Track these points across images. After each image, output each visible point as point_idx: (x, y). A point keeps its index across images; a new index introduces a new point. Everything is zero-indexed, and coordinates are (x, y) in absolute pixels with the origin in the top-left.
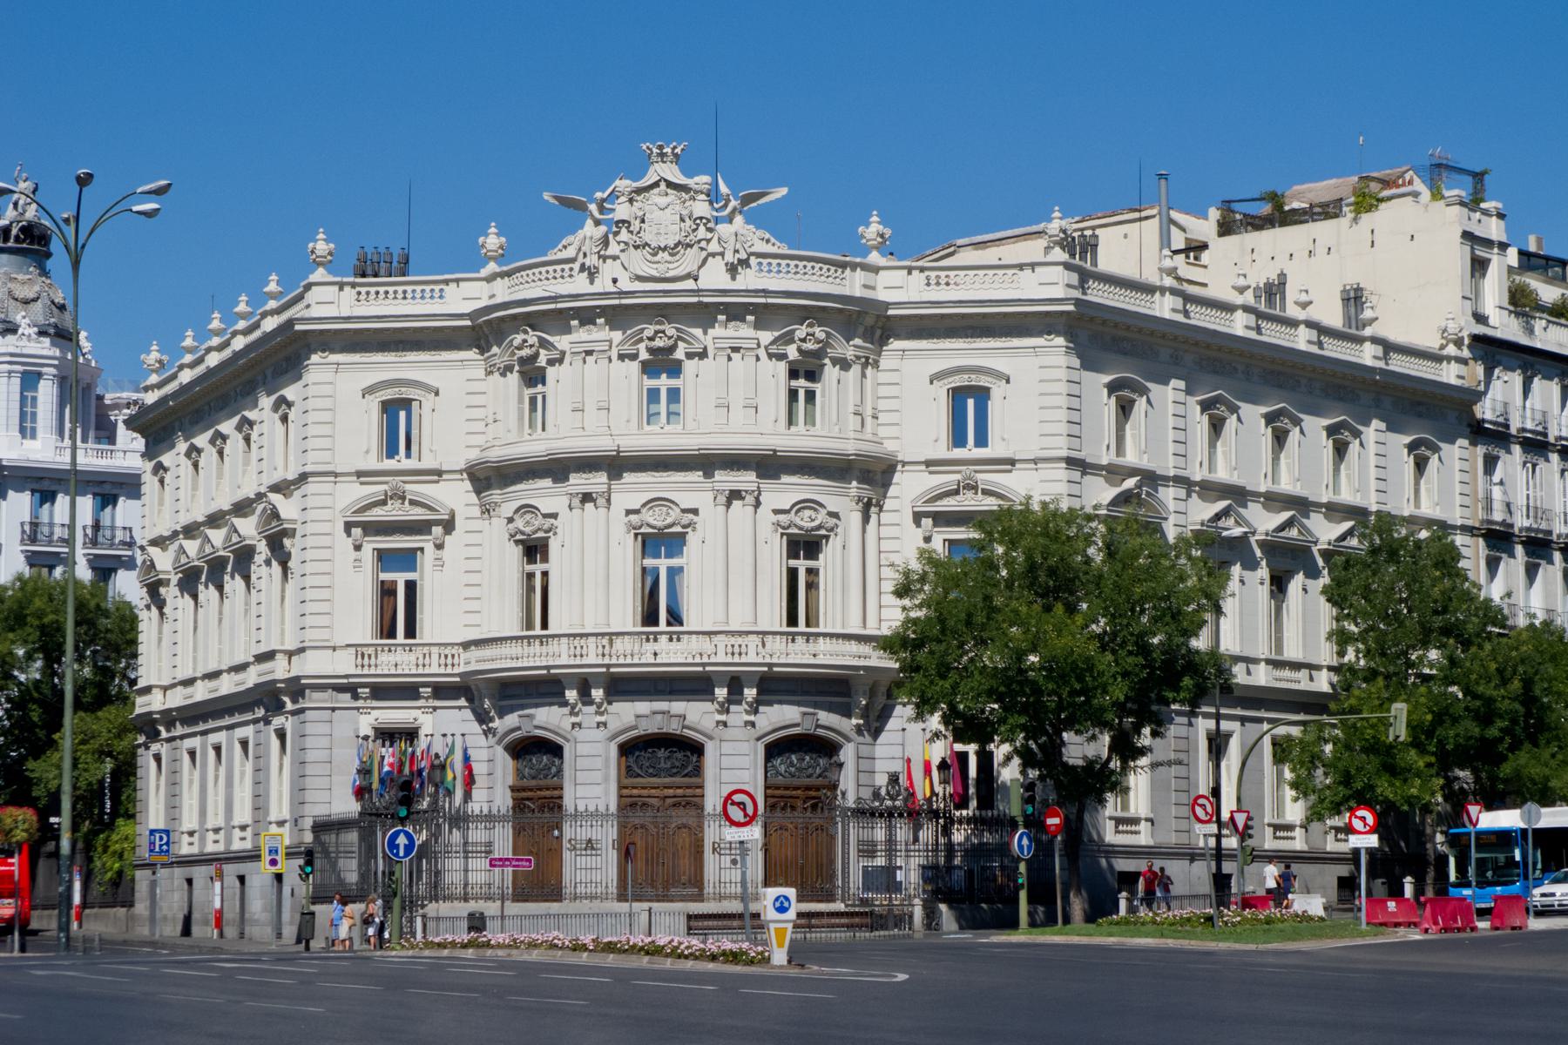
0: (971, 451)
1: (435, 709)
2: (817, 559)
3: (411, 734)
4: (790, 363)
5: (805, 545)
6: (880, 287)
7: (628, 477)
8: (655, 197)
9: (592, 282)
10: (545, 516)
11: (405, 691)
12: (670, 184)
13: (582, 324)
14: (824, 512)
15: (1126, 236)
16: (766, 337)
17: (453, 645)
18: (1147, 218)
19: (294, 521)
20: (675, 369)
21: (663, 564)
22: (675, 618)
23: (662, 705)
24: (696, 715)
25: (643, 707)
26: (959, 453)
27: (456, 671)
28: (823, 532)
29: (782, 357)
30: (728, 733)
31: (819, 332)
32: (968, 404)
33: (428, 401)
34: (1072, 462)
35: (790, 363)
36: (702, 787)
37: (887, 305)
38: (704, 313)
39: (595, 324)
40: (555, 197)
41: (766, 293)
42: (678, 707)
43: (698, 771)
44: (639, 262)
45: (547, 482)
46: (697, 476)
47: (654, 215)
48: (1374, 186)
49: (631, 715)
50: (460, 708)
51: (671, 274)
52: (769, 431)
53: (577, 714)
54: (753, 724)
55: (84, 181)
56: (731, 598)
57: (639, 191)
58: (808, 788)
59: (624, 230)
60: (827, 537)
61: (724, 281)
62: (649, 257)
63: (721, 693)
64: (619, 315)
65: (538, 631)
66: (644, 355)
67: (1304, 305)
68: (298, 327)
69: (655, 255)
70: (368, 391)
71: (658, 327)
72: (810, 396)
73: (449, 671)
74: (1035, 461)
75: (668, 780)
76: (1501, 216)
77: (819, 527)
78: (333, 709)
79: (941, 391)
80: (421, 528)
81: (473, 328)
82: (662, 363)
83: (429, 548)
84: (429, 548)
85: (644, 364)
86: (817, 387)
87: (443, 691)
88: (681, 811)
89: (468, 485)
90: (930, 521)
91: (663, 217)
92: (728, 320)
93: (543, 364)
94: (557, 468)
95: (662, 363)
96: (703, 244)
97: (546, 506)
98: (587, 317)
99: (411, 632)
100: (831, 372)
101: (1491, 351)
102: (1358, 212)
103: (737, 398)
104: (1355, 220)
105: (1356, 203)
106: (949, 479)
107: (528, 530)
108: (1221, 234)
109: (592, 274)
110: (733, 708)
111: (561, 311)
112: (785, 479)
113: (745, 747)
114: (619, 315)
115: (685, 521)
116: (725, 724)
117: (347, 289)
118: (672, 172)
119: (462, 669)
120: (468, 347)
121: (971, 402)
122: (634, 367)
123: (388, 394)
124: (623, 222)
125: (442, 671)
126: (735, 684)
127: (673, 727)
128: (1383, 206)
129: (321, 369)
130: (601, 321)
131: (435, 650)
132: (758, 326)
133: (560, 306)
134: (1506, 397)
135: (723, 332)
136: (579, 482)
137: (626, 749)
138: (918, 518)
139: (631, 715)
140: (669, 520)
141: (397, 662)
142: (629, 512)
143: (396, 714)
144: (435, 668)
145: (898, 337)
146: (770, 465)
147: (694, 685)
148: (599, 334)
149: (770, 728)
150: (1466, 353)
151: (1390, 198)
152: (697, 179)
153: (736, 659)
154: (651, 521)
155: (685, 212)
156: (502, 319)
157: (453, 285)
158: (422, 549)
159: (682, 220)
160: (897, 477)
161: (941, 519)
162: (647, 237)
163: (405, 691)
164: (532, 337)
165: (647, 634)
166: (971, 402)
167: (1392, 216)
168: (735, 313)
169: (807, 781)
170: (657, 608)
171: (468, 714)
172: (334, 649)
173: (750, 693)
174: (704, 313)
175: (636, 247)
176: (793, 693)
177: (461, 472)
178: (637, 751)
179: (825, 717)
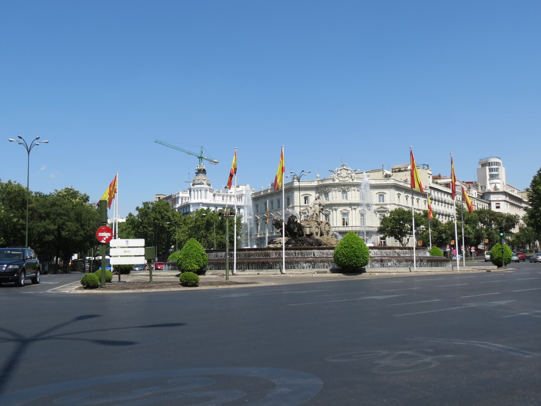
5: (362, 215)
12: (345, 169)
33: (310, 197)
44: (341, 179)
55: (303, 171)
61: (351, 181)
79: (378, 195)
95: (344, 192)
103: (354, 196)
106: (380, 206)
122: (341, 193)
134: (435, 194)
146: (358, 205)
161: (379, 212)
170: (345, 223)
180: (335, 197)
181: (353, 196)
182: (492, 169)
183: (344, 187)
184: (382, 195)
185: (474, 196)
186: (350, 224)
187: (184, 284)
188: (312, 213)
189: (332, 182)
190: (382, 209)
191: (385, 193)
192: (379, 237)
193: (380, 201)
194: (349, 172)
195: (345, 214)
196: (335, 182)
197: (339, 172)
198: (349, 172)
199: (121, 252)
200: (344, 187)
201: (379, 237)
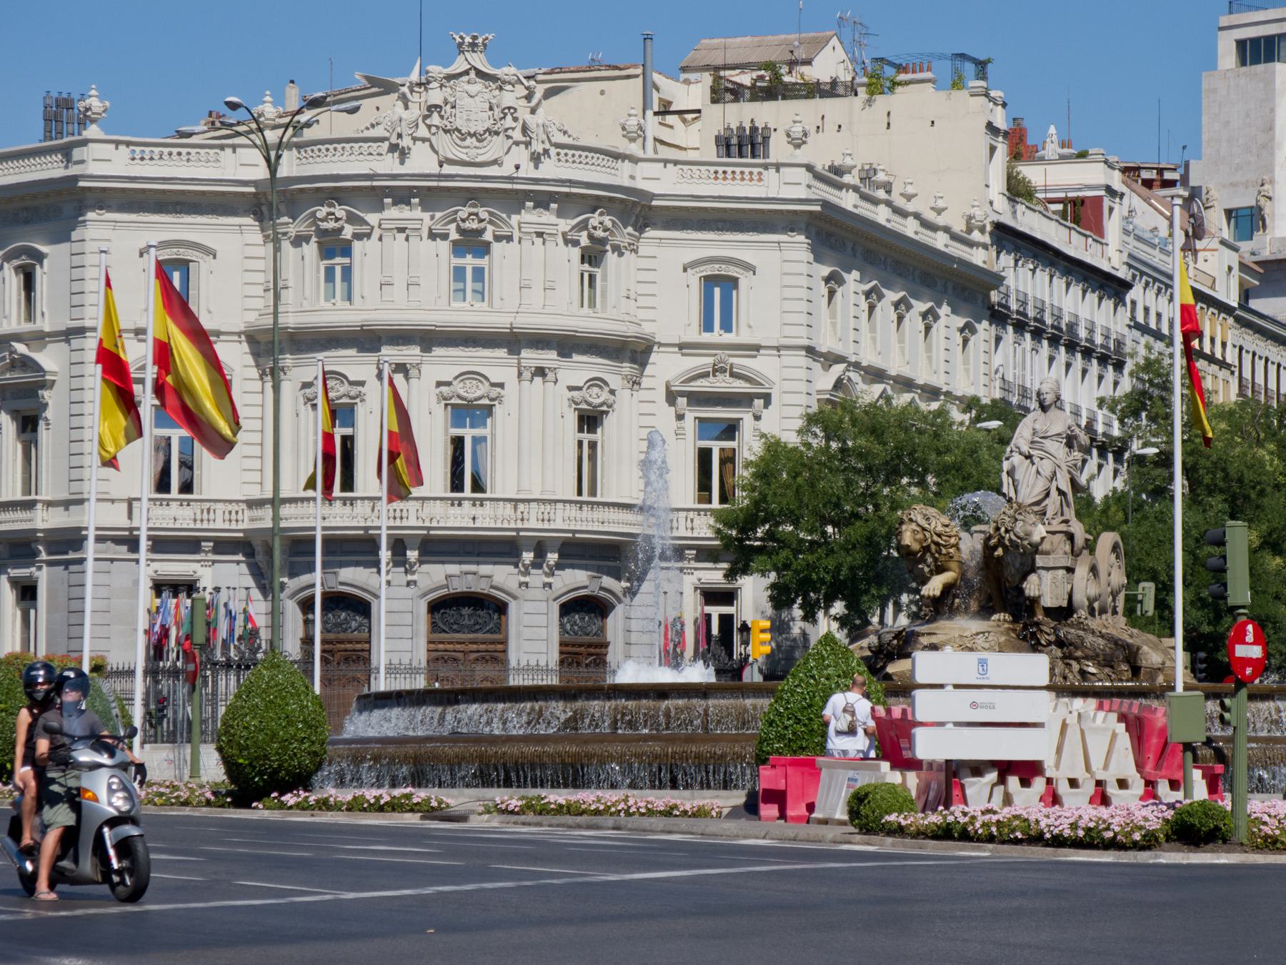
0: (718, 336)
1: (214, 562)
2: (485, 425)
3: (189, 587)
4: (583, 248)
5: (590, 420)
6: (638, 178)
7: (438, 351)
8: (462, 83)
9: (402, 163)
10: (352, 383)
11: (187, 545)
12: (480, 74)
13: (394, 204)
14: (607, 389)
15: (602, 93)
16: (565, 225)
17: (237, 502)
18: (628, 77)
19: (55, 373)
20: (484, 249)
21: (468, 433)
22: (478, 486)
23: (473, 568)
24: (498, 577)
25: (453, 569)
26: (707, 337)
27: (241, 526)
28: (604, 408)
29: (576, 243)
30: (530, 593)
31: (607, 220)
34: (810, 351)
35: (583, 248)
36: (430, 642)
37: (654, 196)
39: (409, 203)
40: (367, 78)
41: (571, 183)
42: (485, 569)
43: (500, 628)
44: (447, 146)
45: (352, 352)
46: (502, 353)
47: (464, 101)
48: (889, 71)
49: (438, 576)
50: (238, 562)
52: (565, 313)
53: (414, 573)
54: (550, 585)
56: (530, 469)
57: (450, 77)
58: (590, 646)
59: (435, 115)
60: (607, 413)
62: (459, 142)
63: (528, 557)
64: (431, 195)
66: (454, 236)
67: (909, 198)
68: (81, 184)
69: (464, 140)
71: (472, 210)
72: (592, 278)
73: (234, 526)
74: (778, 349)
75: (471, 636)
76: (1004, 105)
77: (603, 404)
78: (112, 560)
79: (694, 278)
81: (255, 194)
82: (471, 243)
85: (455, 243)
86: (598, 272)
87: (224, 546)
88: (490, 666)
89: (245, 347)
91: (473, 105)
92: (535, 208)
93: (349, 237)
95: (471, 243)
96: (510, 133)
98: (402, 197)
99: (187, 487)
100: (611, 258)
101: (1006, 237)
102: (872, 93)
104: (869, 102)
105: (869, 85)
106: (705, 362)
108: (714, 101)
109: (404, 154)
110: (533, 571)
111: (373, 188)
112: (576, 357)
113: (542, 607)
114: (431, 195)
115: (493, 395)
116: (527, 584)
117: (122, 148)
118: (478, 60)
119: (246, 525)
120: (245, 213)
121: (717, 291)
122: (444, 247)
123: (165, 255)
124: (436, 106)
125: (227, 526)
126: (540, 548)
127: (481, 587)
128: (899, 89)
129: (99, 229)
130: (416, 201)
131: (220, 506)
132: (560, 214)
133: (375, 183)
134: (1026, 284)
135: (531, 216)
137: (435, 607)
138: (671, 397)
139: (438, 576)
140: (478, 393)
142: (439, 384)
143: (176, 567)
144: (220, 523)
145: (655, 226)
146: (567, 345)
147: (502, 548)
148: (413, 214)
149: (565, 590)
150: (986, 239)
151: (907, 83)
152: (506, 70)
153: (546, 526)
154: (461, 392)
155: (494, 101)
156: (302, 190)
157: (229, 151)
159: (491, 109)
160: (654, 357)
162: (459, 123)
163: (187, 545)
164: (340, 211)
165: (452, 499)
166: (717, 291)
167: (915, 101)
168: (542, 201)
169: (586, 639)
171: (244, 568)
172: (113, 501)
173: (552, 557)
175: (446, 131)
176: (582, 557)
177: (239, 334)
178: (445, 608)
179: (608, 581)
180: (402, 272)
181: (534, 276)
183: (472, 211)
184: (720, 287)
185: (1221, 296)
186: (502, 482)
188: (1041, 485)
189: (388, 165)
190: (722, 384)
191: (750, 268)
192: (689, 581)
193: (708, 326)
194: (510, 97)
195: (470, 412)
196: (412, 166)
197: (435, 96)
198: (510, 97)
201: (689, 581)
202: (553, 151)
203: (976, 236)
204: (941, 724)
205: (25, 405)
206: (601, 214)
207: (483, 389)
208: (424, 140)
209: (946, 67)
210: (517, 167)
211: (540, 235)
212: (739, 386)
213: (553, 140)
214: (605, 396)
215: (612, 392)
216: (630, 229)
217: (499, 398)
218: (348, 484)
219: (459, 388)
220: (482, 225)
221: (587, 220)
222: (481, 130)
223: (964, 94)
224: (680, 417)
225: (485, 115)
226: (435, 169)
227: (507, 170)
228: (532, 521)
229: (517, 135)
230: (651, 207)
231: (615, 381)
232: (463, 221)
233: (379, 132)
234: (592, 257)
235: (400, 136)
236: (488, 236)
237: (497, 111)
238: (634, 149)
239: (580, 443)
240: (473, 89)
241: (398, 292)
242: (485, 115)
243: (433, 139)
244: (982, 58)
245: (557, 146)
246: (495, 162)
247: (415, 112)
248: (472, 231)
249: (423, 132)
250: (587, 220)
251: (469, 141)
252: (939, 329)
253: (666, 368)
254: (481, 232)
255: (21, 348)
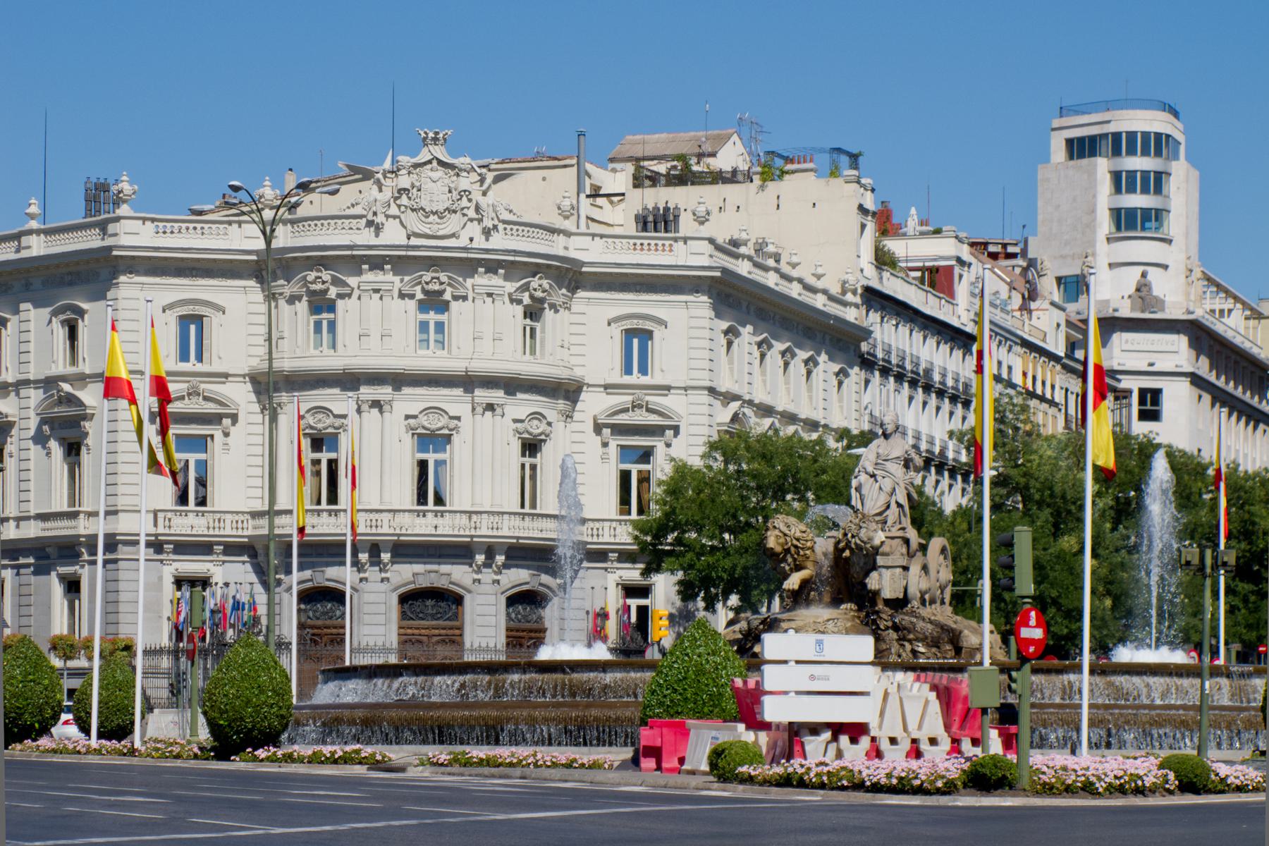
0: (635, 378)
1: (224, 562)
2: (445, 451)
4: (526, 306)
5: (531, 447)
6: (571, 249)
7: (406, 390)
9: (377, 236)
10: (336, 416)
12: (441, 163)
13: (371, 269)
15: (544, 179)
16: (511, 287)
17: (243, 513)
18: (565, 166)
19: (94, 408)
21: (431, 458)
22: (439, 500)
23: (435, 567)
24: (456, 574)
25: (419, 568)
26: (627, 380)
27: (246, 533)
28: (543, 437)
29: (519, 302)
31: (545, 283)
32: (638, 339)
34: (712, 391)
35: (526, 306)
36: (400, 628)
37: (583, 264)
38: (467, 266)
39: (382, 269)
40: (348, 166)
41: (516, 253)
42: (445, 568)
43: (457, 616)
45: (336, 391)
46: (459, 392)
47: (427, 185)
48: (779, 162)
49: (407, 574)
50: (244, 562)
51: (440, 233)
53: (386, 571)
54: (498, 582)
56: (483, 487)
57: (416, 166)
58: (531, 631)
59: (404, 197)
60: (545, 441)
63: (480, 558)
64: (401, 263)
65: (324, 505)
66: (420, 296)
67: (794, 266)
68: (115, 253)
70: (171, 306)
72: (533, 330)
73: (240, 533)
74: (686, 389)
75: (434, 622)
76: (873, 190)
79: (617, 331)
80: (214, 419)
81: (257, 262)
82: (434, 302)
83: (218, 435)
84: (218, 435)
85: (420, 301)
86: (538, 326)
87: (232, 549)
88: (448, 647)
89: (249, 386)
90: (609, 430)
91: (435, 188)
92: (486, 272)
93: (333, 297)
94: (349, 380)
95: (434, 302)
96: (465, 211)
97: (337, 408)
98: (377, 264)
99: (202, 502)
100: (548, 314)
101: (874, 298)
102: (764, 180)
104: (762, 187)
105: (762, 174)
107: (320, 426)
108: (635, 186)
109: (378, 229)
110: (484, 570)
111: (353, 257)
112: (520, 396)
113: (492, 599)
114: (401, 263)
116: (479, 581)
117: (148, 223)
118: (440, 152)
119: (249, 533)
120: (249, 277)
121: (635, 341)
122: (411, 305)
123: (185, 310)
124: (405, 190)
125: (234, 533)
126: (490, 551)
127: (442, 583)
128: (787, 177)
130: (388, 267)
131: (228, 517)
132: (507, 278)
133: (355, 253)
134: (891, 337)
135: (482, 280)
136: (367, 392)
137: (405, 599)
138: (598, 428)
139: (407, 574)
140: (440, 425)
141: (191, 524)
142: (407, 417)
143: (193, 566)
144: (229, 530)
145: (585, 288)
146: (513, 385)
147: (459, 552)
148: (386, 278)
150: (858, 300)
152: (462, 160)
153: (495, 533)
154: (426, 424)
156: (295, 258)
157: (235, 226)
158: (212, 436)
159: (450, 191)
160: (583, 396)
161: (619, 430)
162: (424, 203)
164: (326, 275)
165: (418, 512)
166: (635, 341)
167: (800, 187)
169: (528, 626)
171: (248, 567)
173: (500, 559)
174: (467, 266)
175: (413, 210)
176: (524, 558)
177: (244, 376)
178: (411, 599)
179: (545, 578)
180: (378, 325)
181: (485, 329)
182: (1132, 174)
184: (638, 339)
185: (1050, 347)
186: (459, 498)
187: (1188, 786)
188: (883, 499)
189: (365, 237)
193: (628, 370)
194: (465, 182)
195: (433, 440)
197: (404, 181)
199: (796, 677)
200: (436, 276)
202: (501, 226)
203: (849, 297)
204: (786, 693)
205: (71, 434)
206: (540, 278)
207: (444, 421)
208: (395, 217)
209: (825, 159)
210: (471, 240)
211: (490, 295)
212: (653, 420)
213: (501, 217)
214: (543, 427)
215: (549, 424)
216: (564, 291)
217: (456, 428)
218: (333, 499)
219: (423, 420)
220: (443, 287)
221: (529, 283)
222: (441, 209)
223: (840, 180)
224: (605, 445)
225: (445, 197)
226: (404, 241)
227: (463, 242)
228: (484, 530)
229: (471, 213)
230: (581, 273)
231: (551, 415)
232: (427, 283)
233: (358, 210)
234: (533, 313)
235: (375, 214)
236: (447, 296)
237: (455, 193)
238: (569, 225)
239: (523, 466)
240: (435, 175)
241: (374, 341)
242: (445, 197)
243: (403, 216)
244: (855, 151)
245: (505, 222)
246: (453, 235)
247: (387, 194)
248: (435, 292)
249: (394, 210)
250: (529, 283)
251: (432, 218)
252: (818, 373)
253: (593, 404)
254: (441, 293)
255: (66, 387)
